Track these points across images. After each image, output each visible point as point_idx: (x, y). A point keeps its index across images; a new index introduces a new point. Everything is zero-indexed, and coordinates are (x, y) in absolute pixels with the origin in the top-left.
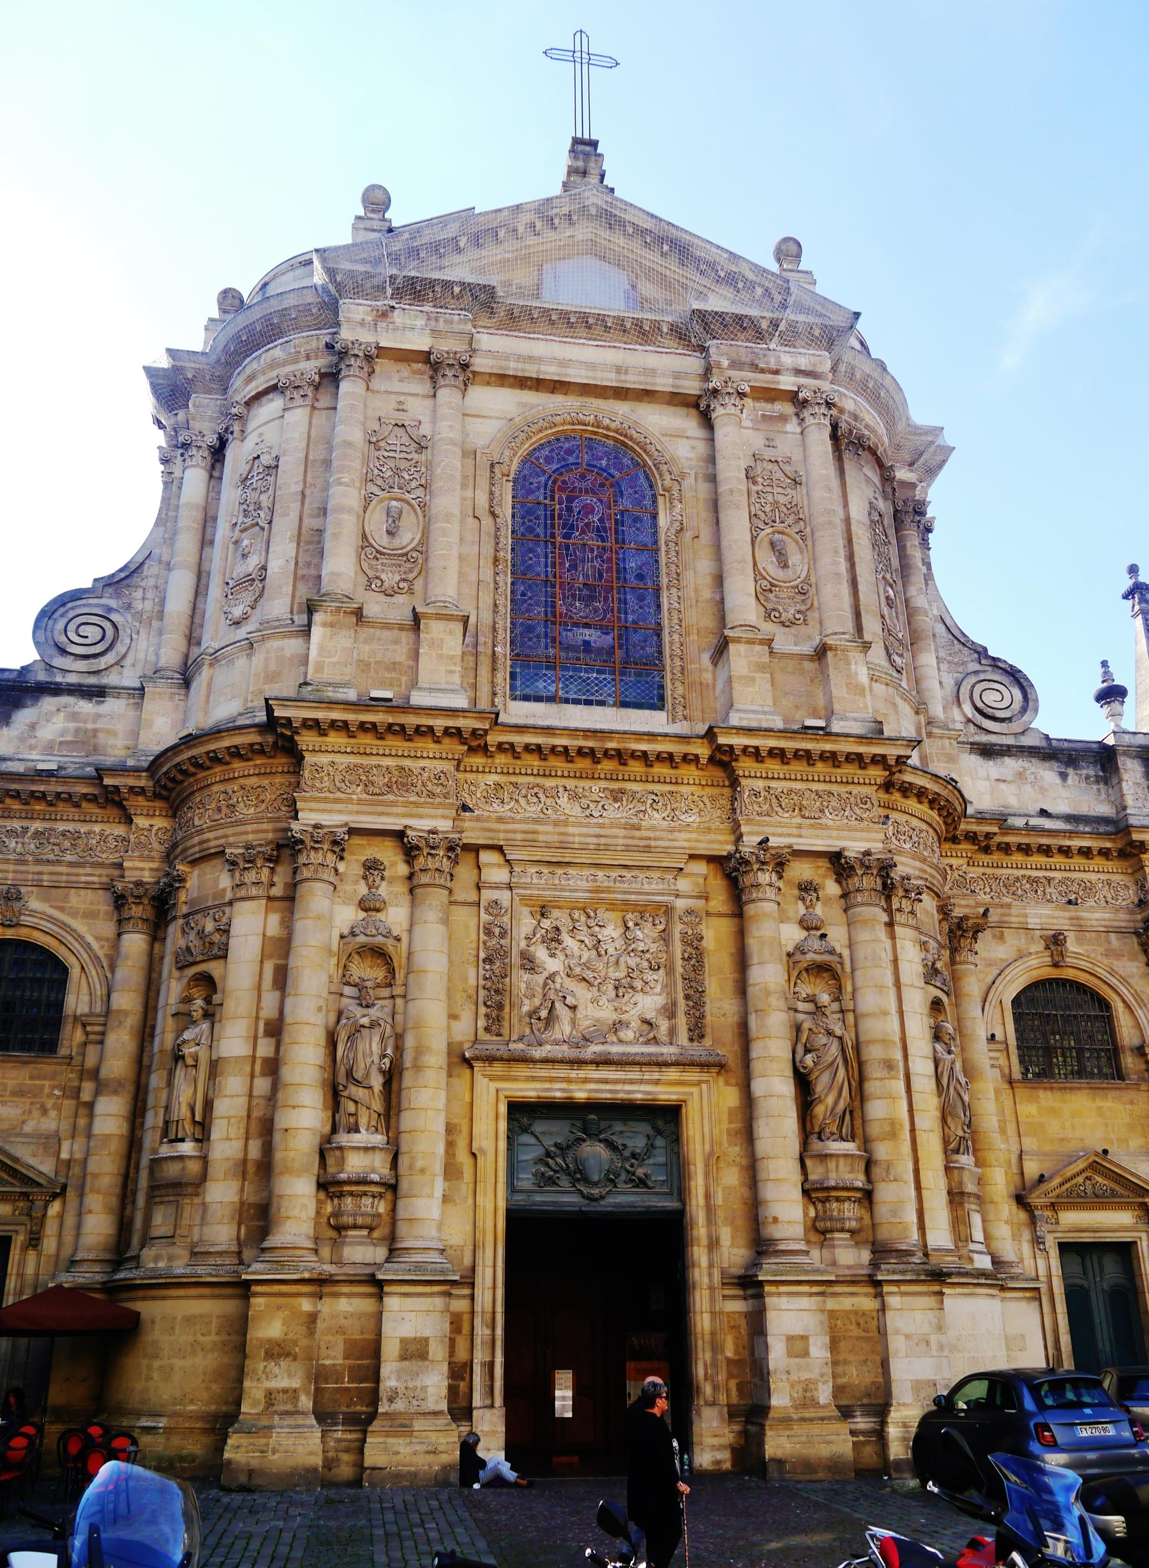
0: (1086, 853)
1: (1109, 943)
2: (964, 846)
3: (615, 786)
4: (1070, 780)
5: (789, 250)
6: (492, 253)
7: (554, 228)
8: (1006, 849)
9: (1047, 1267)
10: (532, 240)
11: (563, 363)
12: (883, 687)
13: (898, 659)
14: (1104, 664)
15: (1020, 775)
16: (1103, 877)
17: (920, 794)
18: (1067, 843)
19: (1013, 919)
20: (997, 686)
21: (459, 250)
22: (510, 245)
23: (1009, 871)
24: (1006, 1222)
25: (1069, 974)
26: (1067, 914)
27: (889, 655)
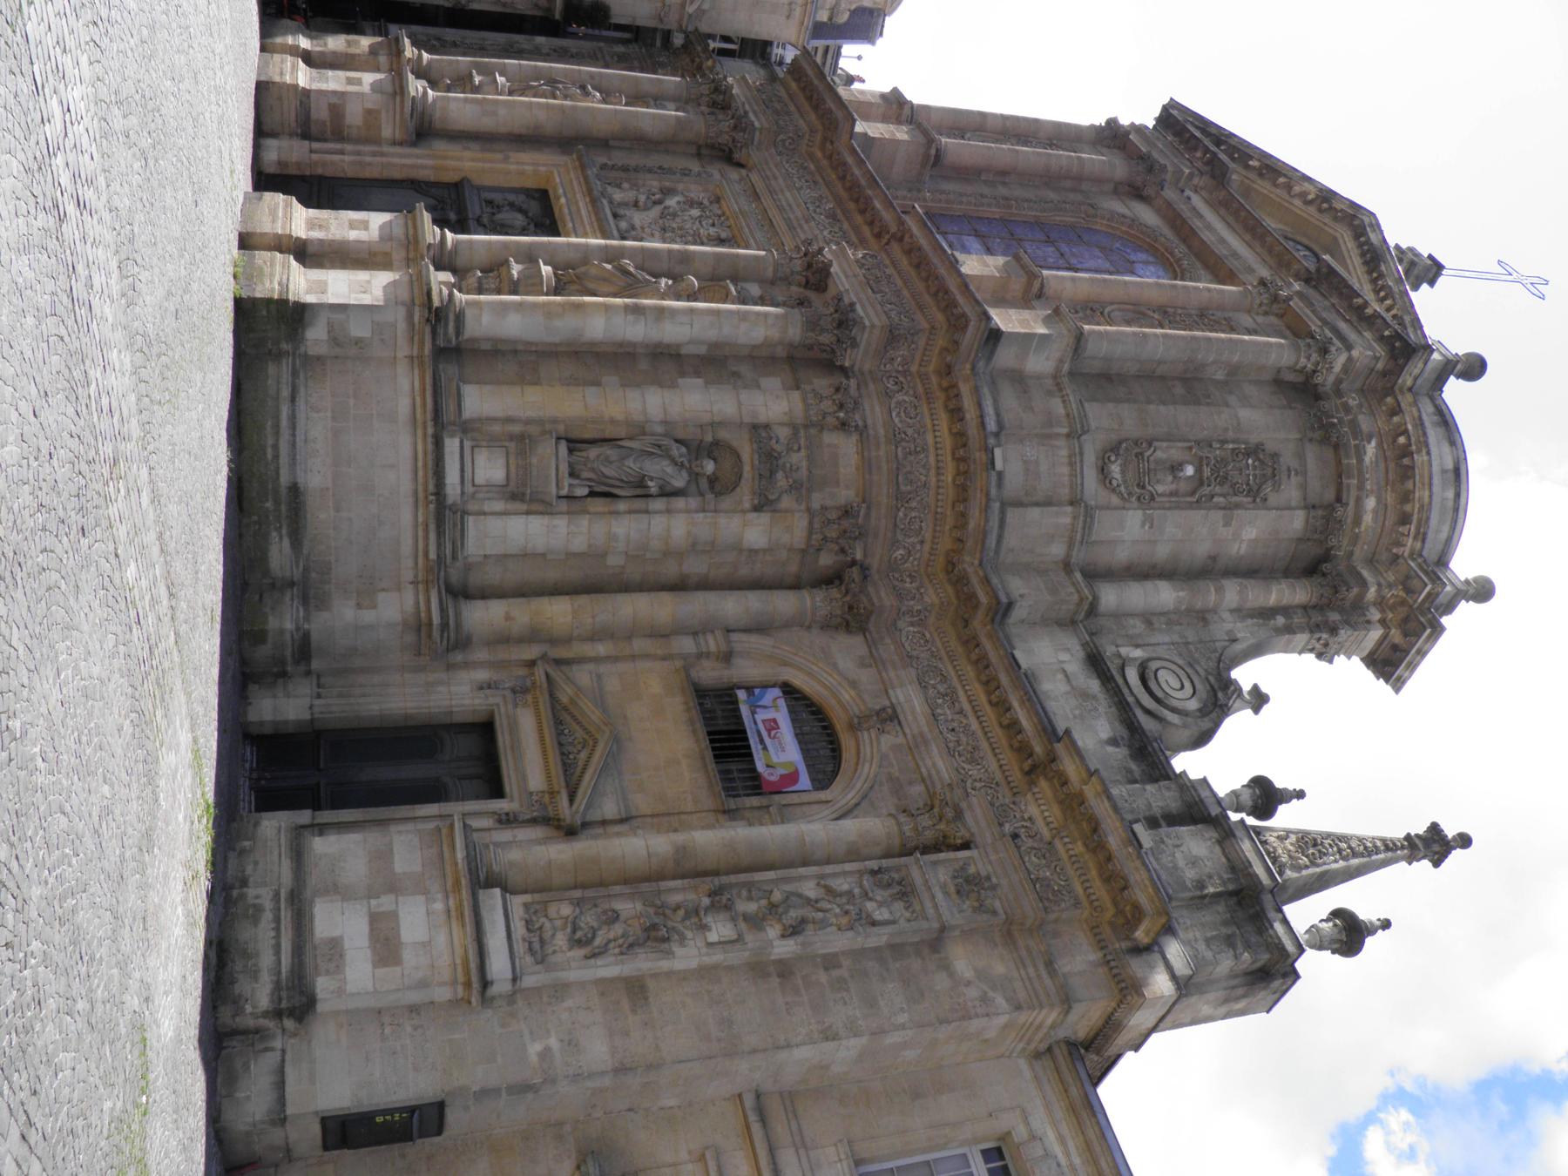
0: (1013, 727)
1: (910, 783)
2: (950, 589)
3: (840, 216)
4: (1110, 749)
5: (1473, 368)
6: (1263, 186)
7: (1320, 210)
8: (971, 643)
9: (457, 694)
10: (1297, 202)
11: (1209, 227)
12: (1062, 411)
13: (1115, 469)
14: (1300, 795)
15: (1085, 695)
16: (998, 776)
17: (956, 413)
18: (1016, 704)
19: (892, 674)
20: (1187, 684)
21: (1247, 167)
22: (1282, 193)
23: (953, 673)
24: (508, 618)
25: (846, 741)
26: (926, 729)
27: (1115, 448)
